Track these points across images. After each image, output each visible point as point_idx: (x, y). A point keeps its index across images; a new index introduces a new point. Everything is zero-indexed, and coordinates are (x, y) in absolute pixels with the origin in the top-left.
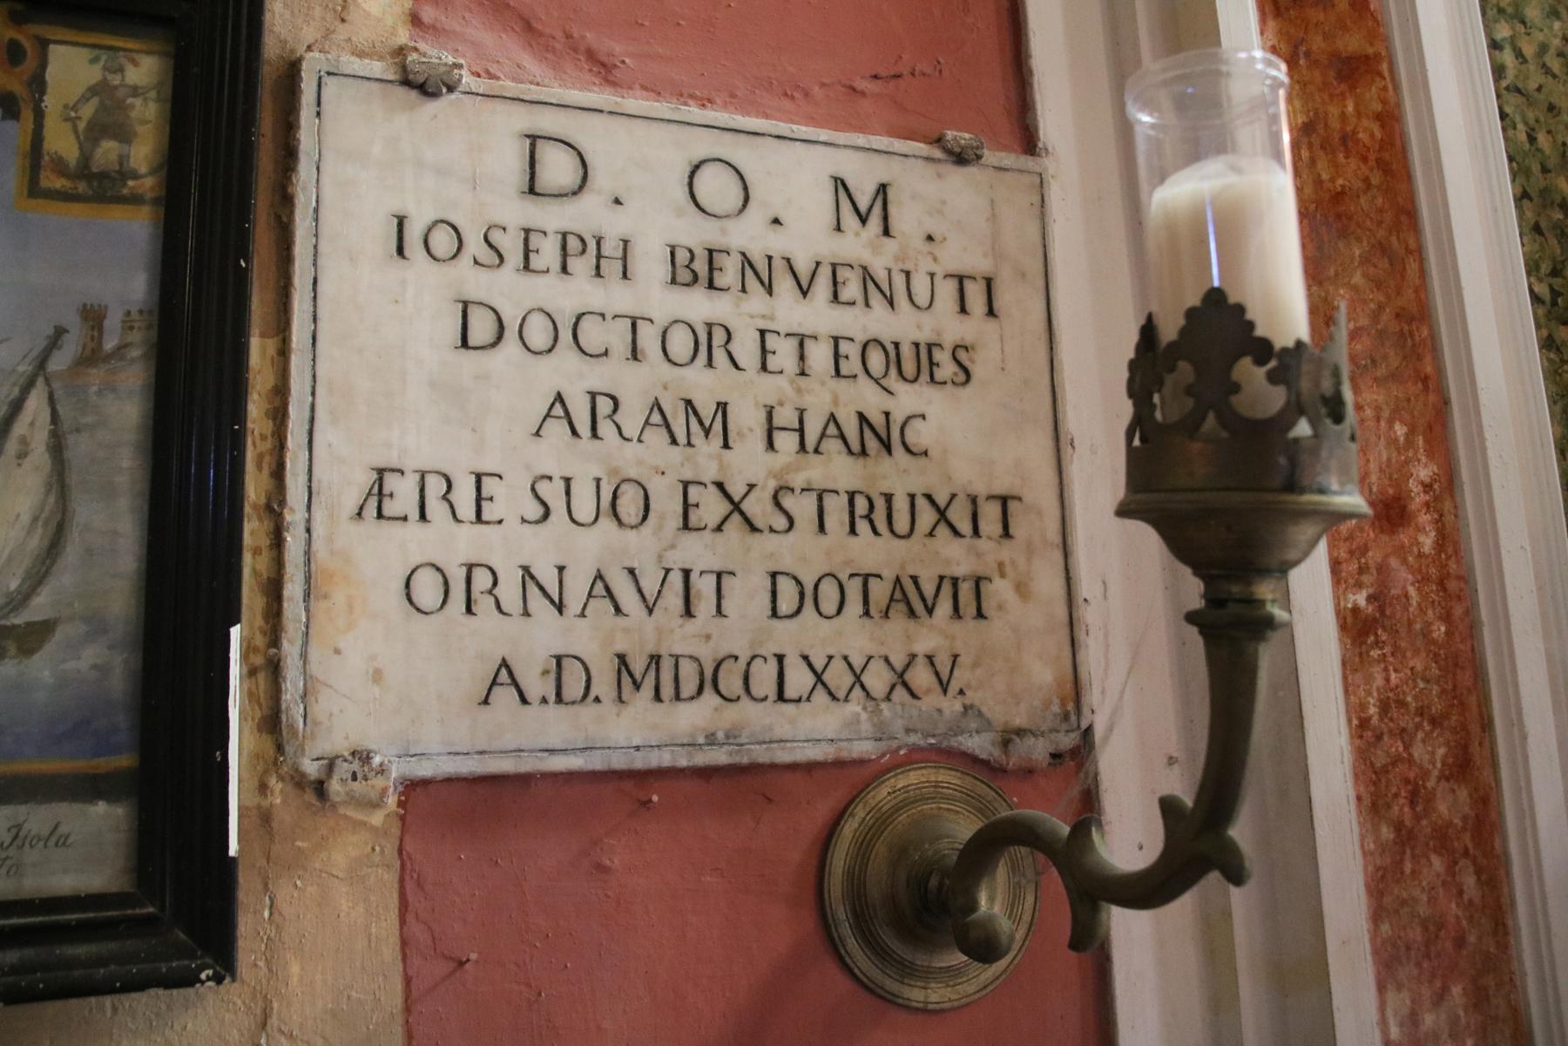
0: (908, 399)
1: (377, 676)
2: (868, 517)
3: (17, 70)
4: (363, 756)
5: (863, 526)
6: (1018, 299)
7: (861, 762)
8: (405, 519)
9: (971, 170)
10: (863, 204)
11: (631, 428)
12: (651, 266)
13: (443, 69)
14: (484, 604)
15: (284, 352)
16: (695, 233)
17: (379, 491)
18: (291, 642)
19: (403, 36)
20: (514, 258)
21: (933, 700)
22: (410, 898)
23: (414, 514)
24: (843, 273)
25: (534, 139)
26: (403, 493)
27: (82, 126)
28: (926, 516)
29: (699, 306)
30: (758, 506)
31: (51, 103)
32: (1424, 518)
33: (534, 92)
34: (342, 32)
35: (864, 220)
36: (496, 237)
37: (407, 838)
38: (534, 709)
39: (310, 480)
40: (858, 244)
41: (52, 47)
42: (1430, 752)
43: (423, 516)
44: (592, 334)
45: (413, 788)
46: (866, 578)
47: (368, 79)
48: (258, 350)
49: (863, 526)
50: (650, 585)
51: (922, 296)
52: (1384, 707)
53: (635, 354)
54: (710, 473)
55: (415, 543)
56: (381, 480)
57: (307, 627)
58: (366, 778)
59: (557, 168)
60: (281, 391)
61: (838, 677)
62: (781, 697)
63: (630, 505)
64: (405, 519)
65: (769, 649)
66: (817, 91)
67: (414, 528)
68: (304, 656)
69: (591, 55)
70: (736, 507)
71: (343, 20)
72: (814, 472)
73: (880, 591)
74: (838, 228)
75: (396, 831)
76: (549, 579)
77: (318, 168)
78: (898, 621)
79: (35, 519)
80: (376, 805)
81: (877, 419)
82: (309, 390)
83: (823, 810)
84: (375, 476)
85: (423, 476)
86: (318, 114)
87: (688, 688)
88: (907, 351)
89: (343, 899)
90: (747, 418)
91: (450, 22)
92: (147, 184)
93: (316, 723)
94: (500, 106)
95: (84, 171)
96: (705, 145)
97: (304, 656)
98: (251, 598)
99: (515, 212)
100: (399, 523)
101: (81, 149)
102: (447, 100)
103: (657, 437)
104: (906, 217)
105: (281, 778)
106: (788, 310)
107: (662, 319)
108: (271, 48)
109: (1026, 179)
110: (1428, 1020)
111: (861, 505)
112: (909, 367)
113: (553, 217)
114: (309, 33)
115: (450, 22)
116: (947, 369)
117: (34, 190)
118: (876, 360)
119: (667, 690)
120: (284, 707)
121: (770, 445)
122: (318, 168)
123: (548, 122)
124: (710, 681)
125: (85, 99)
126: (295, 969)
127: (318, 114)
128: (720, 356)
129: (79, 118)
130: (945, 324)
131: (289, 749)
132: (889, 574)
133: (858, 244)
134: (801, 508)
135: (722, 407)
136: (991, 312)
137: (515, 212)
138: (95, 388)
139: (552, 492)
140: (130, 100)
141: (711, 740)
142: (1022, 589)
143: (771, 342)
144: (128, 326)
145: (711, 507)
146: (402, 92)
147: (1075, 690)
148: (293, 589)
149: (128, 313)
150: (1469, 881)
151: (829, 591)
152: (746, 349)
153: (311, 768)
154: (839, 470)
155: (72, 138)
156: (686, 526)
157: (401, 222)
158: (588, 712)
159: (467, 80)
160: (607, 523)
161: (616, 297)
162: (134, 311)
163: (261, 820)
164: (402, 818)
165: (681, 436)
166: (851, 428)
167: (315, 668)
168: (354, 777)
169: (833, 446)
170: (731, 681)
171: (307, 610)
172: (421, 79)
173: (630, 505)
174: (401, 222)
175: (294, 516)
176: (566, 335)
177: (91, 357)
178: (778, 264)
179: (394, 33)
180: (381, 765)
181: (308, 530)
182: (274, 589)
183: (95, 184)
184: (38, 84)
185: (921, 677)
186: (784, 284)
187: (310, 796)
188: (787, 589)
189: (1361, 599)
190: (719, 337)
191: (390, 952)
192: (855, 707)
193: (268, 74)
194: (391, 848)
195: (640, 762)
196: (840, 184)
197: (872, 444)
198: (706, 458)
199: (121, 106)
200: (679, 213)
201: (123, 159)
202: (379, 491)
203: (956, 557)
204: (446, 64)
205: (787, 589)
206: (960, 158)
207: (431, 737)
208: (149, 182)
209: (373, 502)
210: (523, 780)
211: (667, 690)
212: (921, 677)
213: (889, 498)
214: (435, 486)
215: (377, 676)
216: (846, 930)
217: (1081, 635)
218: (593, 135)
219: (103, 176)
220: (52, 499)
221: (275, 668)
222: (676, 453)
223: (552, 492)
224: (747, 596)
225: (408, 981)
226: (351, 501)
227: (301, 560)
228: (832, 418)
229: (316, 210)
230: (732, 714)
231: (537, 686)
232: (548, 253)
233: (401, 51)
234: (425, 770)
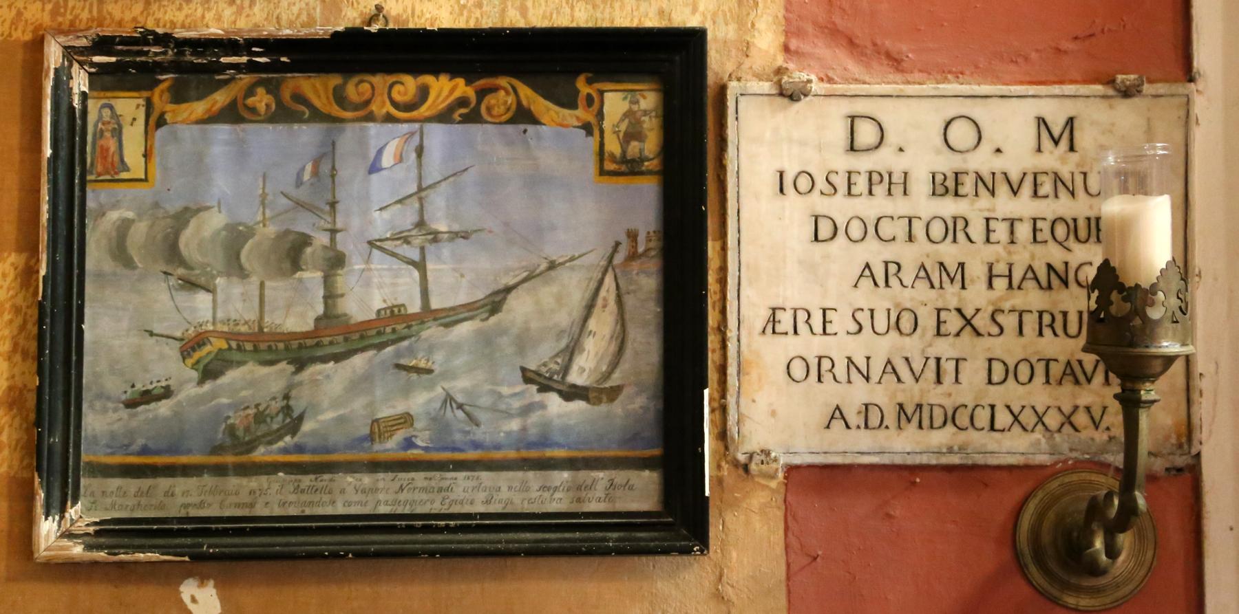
1: (773, 413)
2: (1051, 326)
3: (591, 109)
4: (767, 453)
5: (1047, 332)
7: (1041, 467)
8: (786, 333)
9: (1136, 101)
10: (1056, 132)
11: (908, 281)
12: (921, 186)
13: (801, 85)
14: (827, 377)
15: (724, 248)
16: (946, 163)
17: (773, 320)
18: (731, 396)
19: (780, 61)
20: (842, 189)
21: (1088, 433)
22: (790, 524)
23: (791, 331)
24: (1040, 179)
25: (853, 118)
27: (621, 135)
29: (949, 207)
30: (981, 322)
31: (607, 124)
33: (854, 88)
34: (747, 63)
35: (1056, 142)
36: (833, 178)
37: (788, 495)
38: (853, 431)
39: (739, 315)
40: (1053, 158)
41: (606, 94)
43: (796, 332)
44: (886, 229)
45: (791, 469)
46: (1048, 361)
47: (762, 95)
48: (712, 248)
49: (1047, 332)
50: (917, 366)
53: (911, 238)
54: (953, 303)
56: (774, 314)
57: (739, 388)
58: (768, 463)
59: (866, 133)
60: (723, 269)
61: (1028, 418)
62: (992, 428)
63: (906, 324)
64: (786, 333)
65: (986, 402)
66: (1034, 55)
67: (791, 338)
68: (738, 403)
69: (888, 55)
70: (968, 322)
71: (747, 56)
72: (1017, 300)
73: (1056, 369)
74: (1039, 150)
75: (783, 490)
76: (862, 365)
77: (738, 149)
78: (1068, 387)
79: (612, 337)
80: (772, 477)
81: (1060, 267)
82: (737, 269)
83: (1018, 493)
84: (771, 312)
85: (795, 310)
86: (737, 119)
87: (938, 421)
88: (1082, 224)
89: (757, 523)
90: (977, 270)
91: (806, 47)
92: (653, 165)
93: (744, 437)
94: (833, 101)
95: (624, 160)
96: (953, 108)
97: (738, 403)
98: (713, 375)
99: (843, 162)
100: (784, 336)
101: (622, 147)
102: (805, 100)
103: (922, 285)
104: (1084, 138)
105: (727, 462)
106: (1005, 205)
107: (926, 216)
108: (711, 79)
109: (1176, 101)
111: (1047, 319)
112: (1083, 234)
113: (864, 163)
114: (730, 67)
115: (806, 47)
117: (602, 172)
118: (1061, 231)
119: (926, 422)
120: (728, 427)
121: (990, 286)
122: (738, 149)
123: (860, 107)
124: (950, 418)
125: (622, 120)
126: (734, 554)
127: (737, 119)
128: (961, 236)
129: (620, 131)
131: (731, 448)
132: (1063, 359)
133: (1053, 158)
134: (1009, 321)
135: (962, 265)
137: (843, 162)
138: (635, 272)
139: (864, 318)
140: (643, 118)
141: (950, 450)
143: (993, 224)
144: (649, 240)
145: (953, 322)
146: (780, 100)
148: (732, 370)
149: (649, 233)
151: (1024, 371)
152: (977, 231)
153: (742, 458)
154: (1033, 298)
155: (617, 142)
156: (938, 334)
157: (781, 174)
158: (882, 433)
159: (816, 87)
160: (893, 334)
161: (900, 206)
162: (651, 231)
163: (718, 482)
164: (786, 485)
165: (937, 284)
166: (1042, 273)
167: (743, 409)
168: (762, 463)
169: (1030, 284)
170: (963, 419)
171: (739, 380)
172: (789, 93)
173: (906, 324)
174: (781, 174)
175: (732, 333)
176: (871, 230)
177: (633, 256)
178: (999, 177)
179: (774, 59)
180: (775, 457)
181: (739, 341)
182: (723, 370)
183: (629, 165)
184: (600, 115)
185: (1081, 419)
186: (1003, 190)
187: (741, 471)
188: (998, 369)
190: (960, 225)
191: (779, 549)
192: (1038, 435)
193: (710, 93)
194: (780, 498)
195: (910, 461)
196: (1041, 122)
197: (1055, 282)
198: (951, 295)
199: (639, 123)
200: (938, 152)
201: (641, 151)
202: (773, 320)
204: (803, 82)
205: (998, 369)
207: (800, 444)
208: (655, 162)
209: (770, 326)
210: (848, 468)
211: (926, 422)
212: (1081, 419)
213: (1065, 314)
214: (802, 316)
215: (773, 413)
216: (1028, 559)
217: (1195, 396)
218: (887, 112)
219: (633, 161)
220: (619, 327)
221: (724, 409)
222: (933, 294)
223: (864, 318)
224: (973, 373)
225: (788, 565)
226: (759, 326)
227: (736, 355)
228: (1030, 268)
229: (738, 172)
230: (962, 437)
231: (854, 419)
232: (861, 184)
233: (779, 71)
234: (797, 460)
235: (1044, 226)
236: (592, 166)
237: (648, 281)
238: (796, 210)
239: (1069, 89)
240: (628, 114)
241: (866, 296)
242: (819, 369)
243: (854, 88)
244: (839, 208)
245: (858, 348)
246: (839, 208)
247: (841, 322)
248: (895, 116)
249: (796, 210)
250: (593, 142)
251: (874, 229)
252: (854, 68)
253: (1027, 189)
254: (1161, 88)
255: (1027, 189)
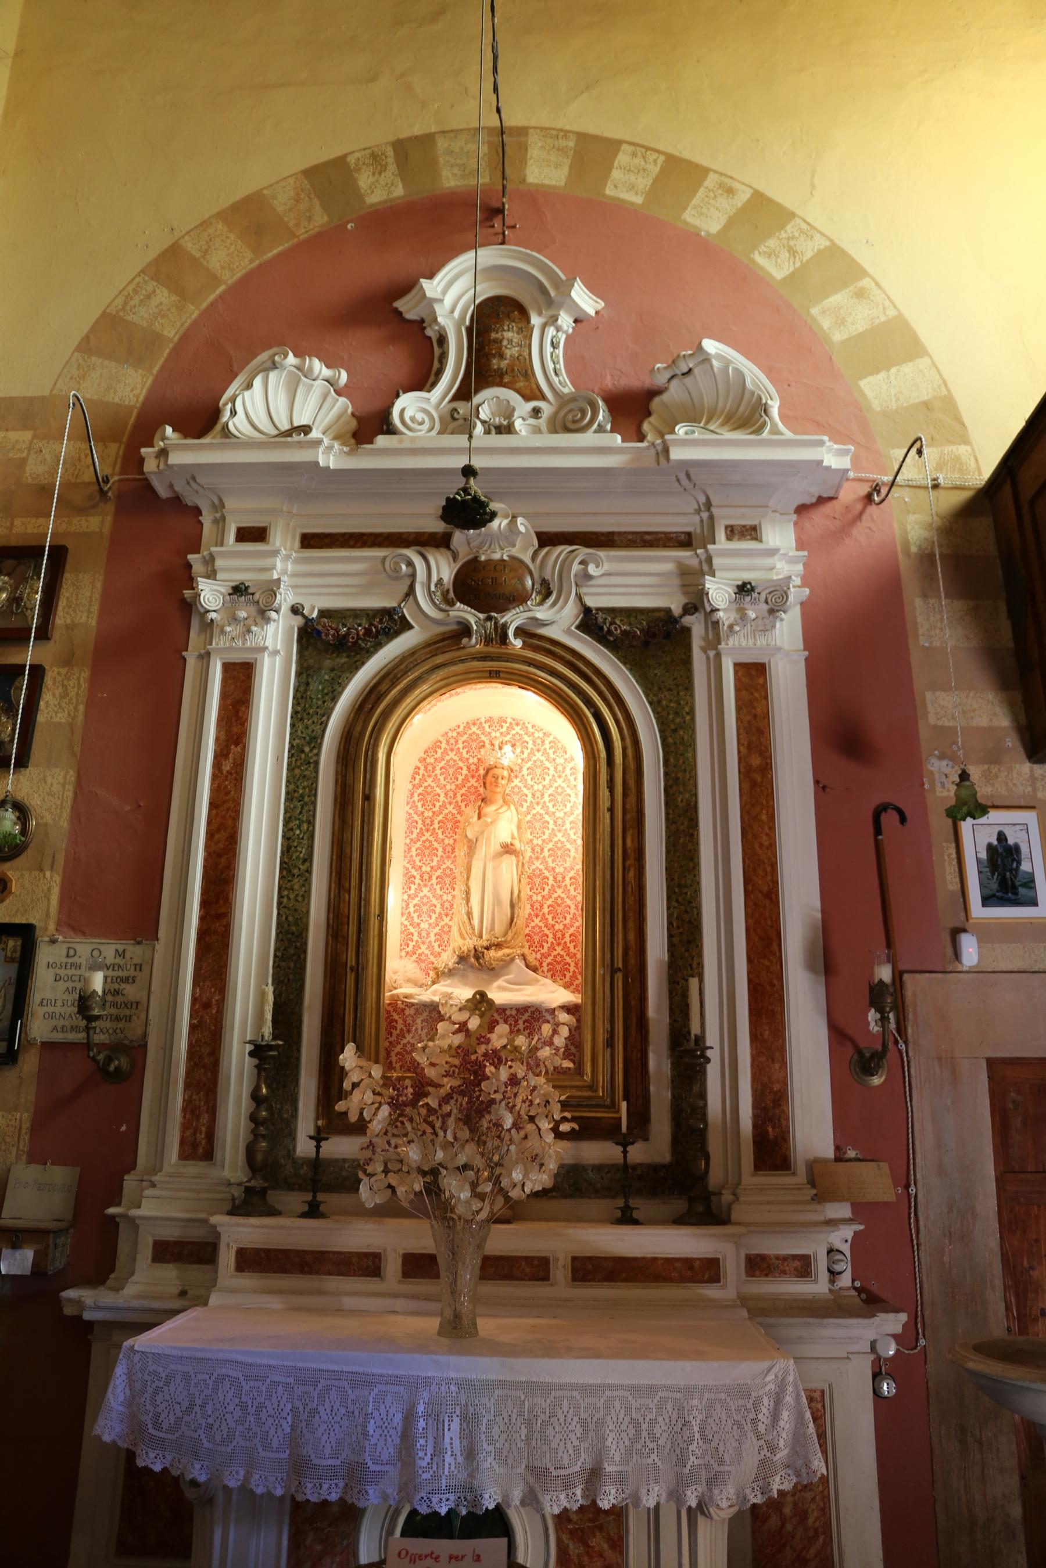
0: (123, 986)
6: (146, 969)
17: (42, 1002)
26: (45, 1002)
28: (123, 1005)
32: (215, 1007)
33: (70, 940)
40: (118, 961)
42: (205, 1050)
44: (74, 978)
45: (42, 1043)
46: (111, 1015)
51: (128, 968)
52: (196, 1041)
53: (80, 981)
55: (46, 1009)
59: (72, 952)
73: (113, 1018)
76: (63, 1014)
78: (116, 1023)
92: (18, 960)
95: (11, 958)
99: (64, 960)
104: (128, 955)
110: (194, 1097)
113: (70, 960)
116: (131, 980)
117: (6, 961)
123: (71, 945)
130: (132, 973)
133: (118, 961)
136: (140, 970)
137: (64, 960)
139: (65, 1002)
142: (138, 1018)
147: (145, 1035)
150: (209, 1075)
161: (78, 972)
166: (112, 991)
177: (9, 984)
185: (118, 1031)
189: (196, 1022)
192: (107, 1035)
196: (117, 950)
202: (42, 1002)
203: (127, 1012)
206: (139, 943)
212: (118, 1031)
218: (78, 947)
223: (65, 1002)
231: (59, 1029)
232: (69, 966)
235: (115, 979)
236: (3, 959)
237: (12, 991)
238: (51, 972)
239: (125, 942)
240: (14, 946)
241: (66, 997)
242: (52, 1016)
243: (70, 940)
244: (62, 972)
245: (63, 1010)
246: (62, 972)
247: (59, 1003)
248: (80, 948)
249: (51, 972)
250: (4, 953)
251: (70, 978)
252: (73, 935)
253: (111, 969)
254: (148, 942)
255: (111, 969)
